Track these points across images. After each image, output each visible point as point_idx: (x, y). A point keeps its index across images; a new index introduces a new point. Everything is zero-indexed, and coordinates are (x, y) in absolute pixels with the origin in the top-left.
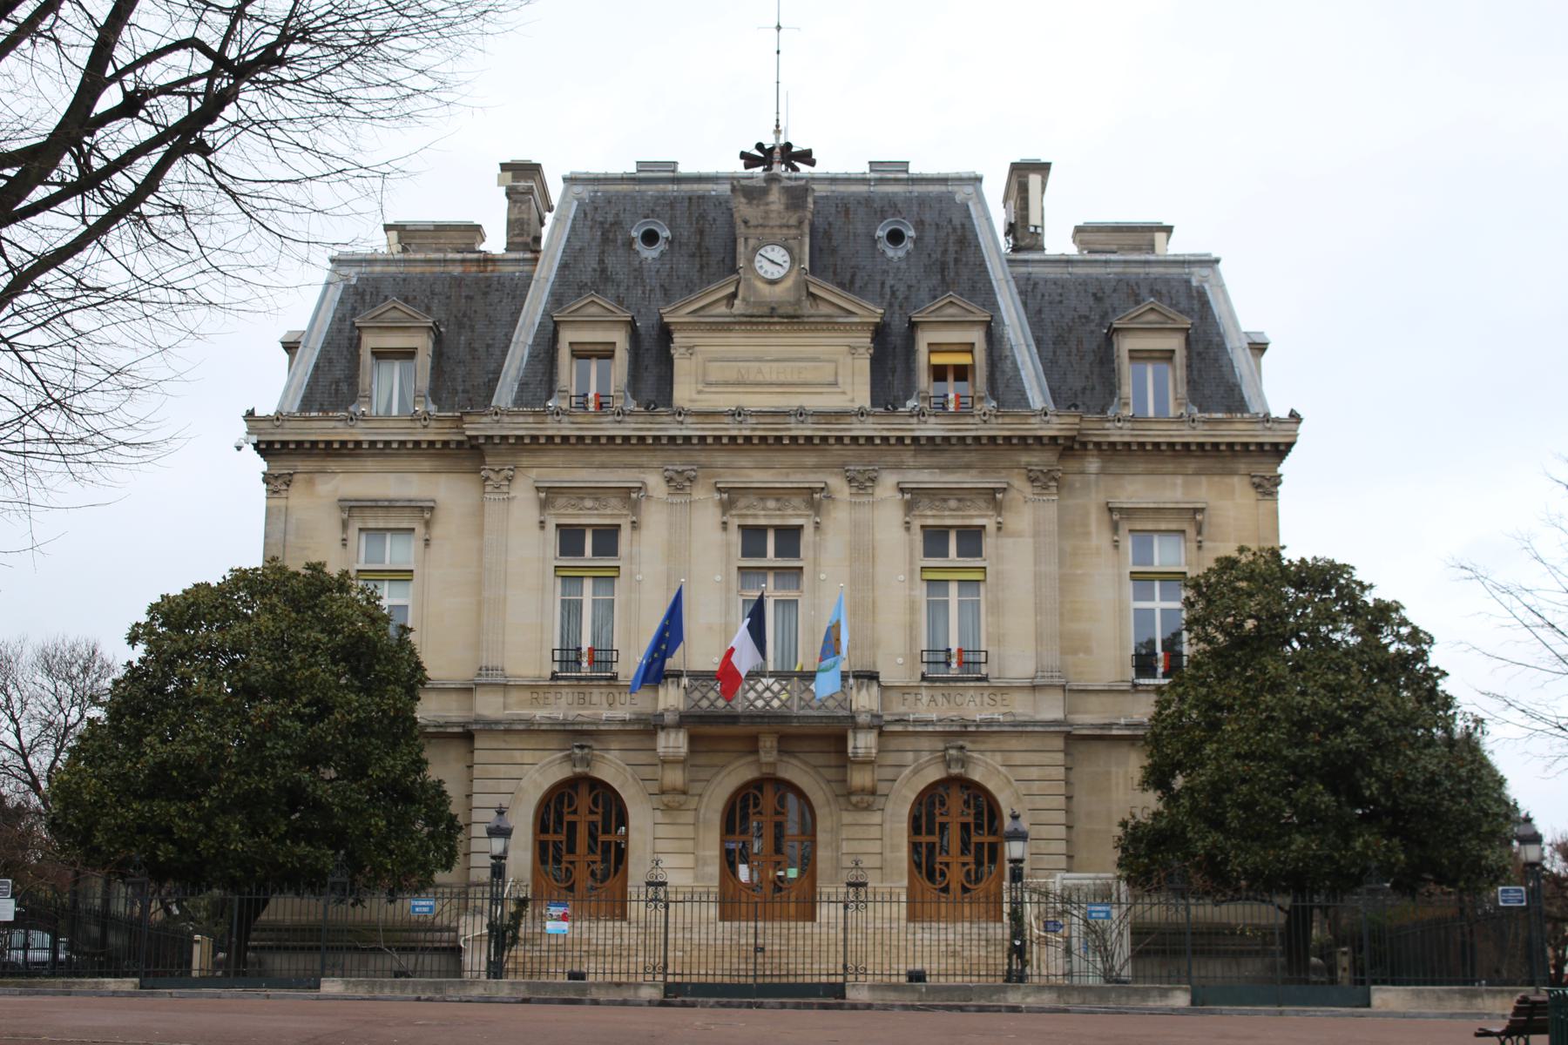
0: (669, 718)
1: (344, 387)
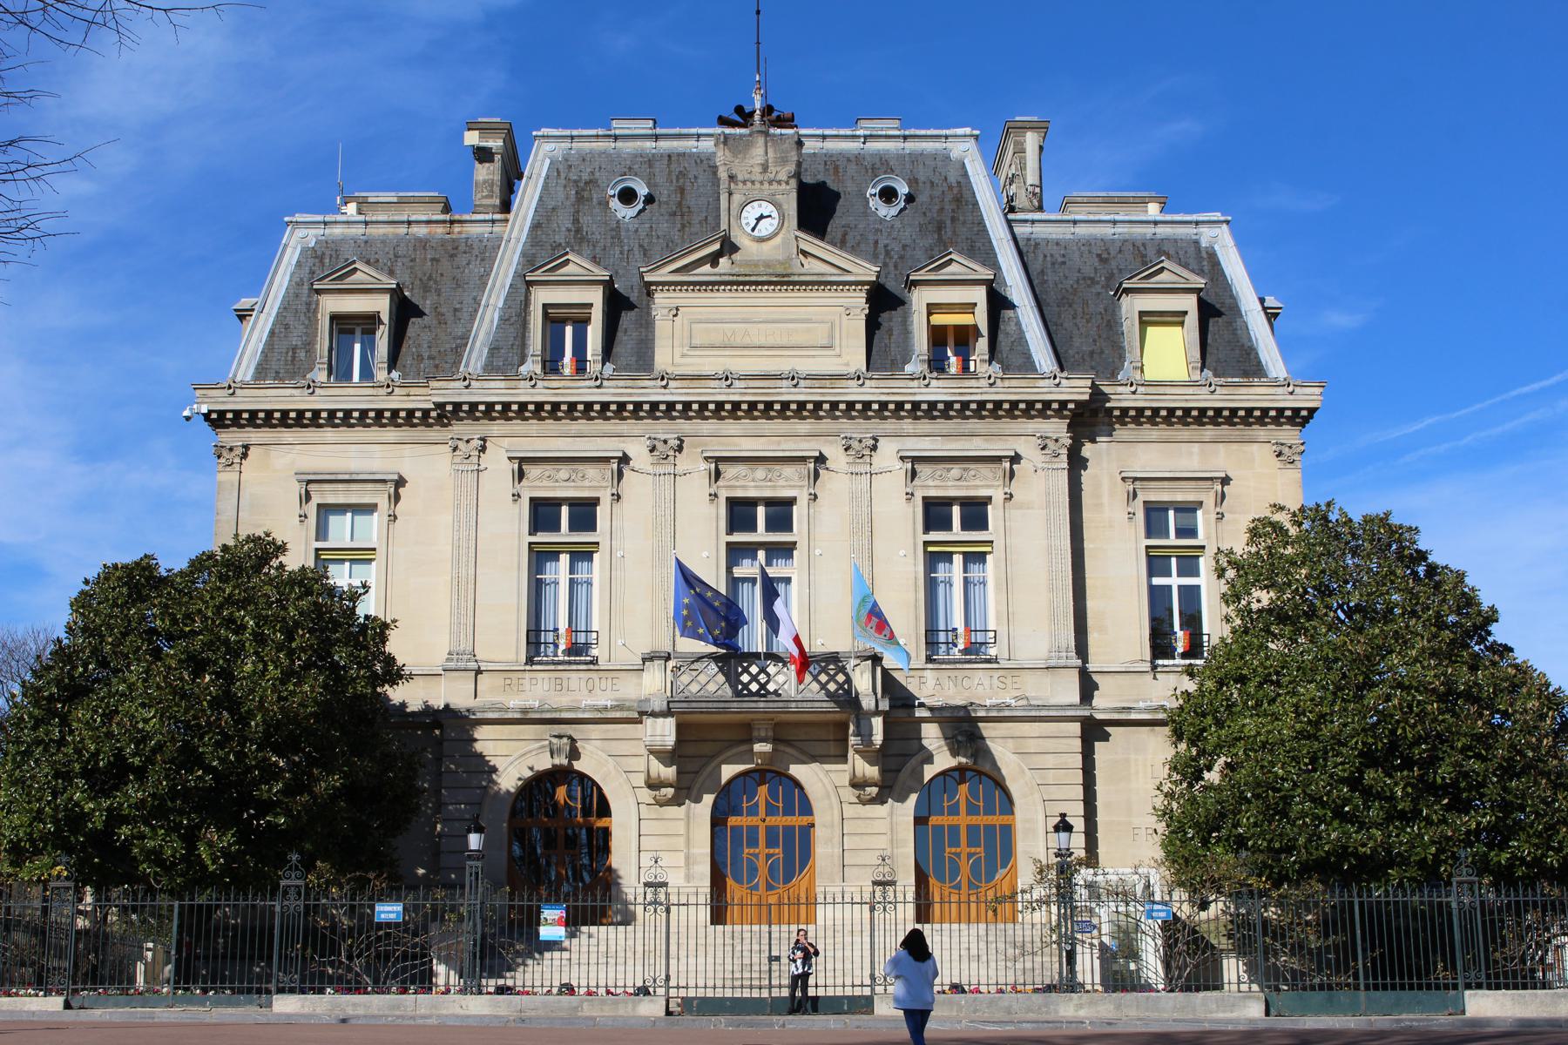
0: (658, 705)
1: (302, 354)
